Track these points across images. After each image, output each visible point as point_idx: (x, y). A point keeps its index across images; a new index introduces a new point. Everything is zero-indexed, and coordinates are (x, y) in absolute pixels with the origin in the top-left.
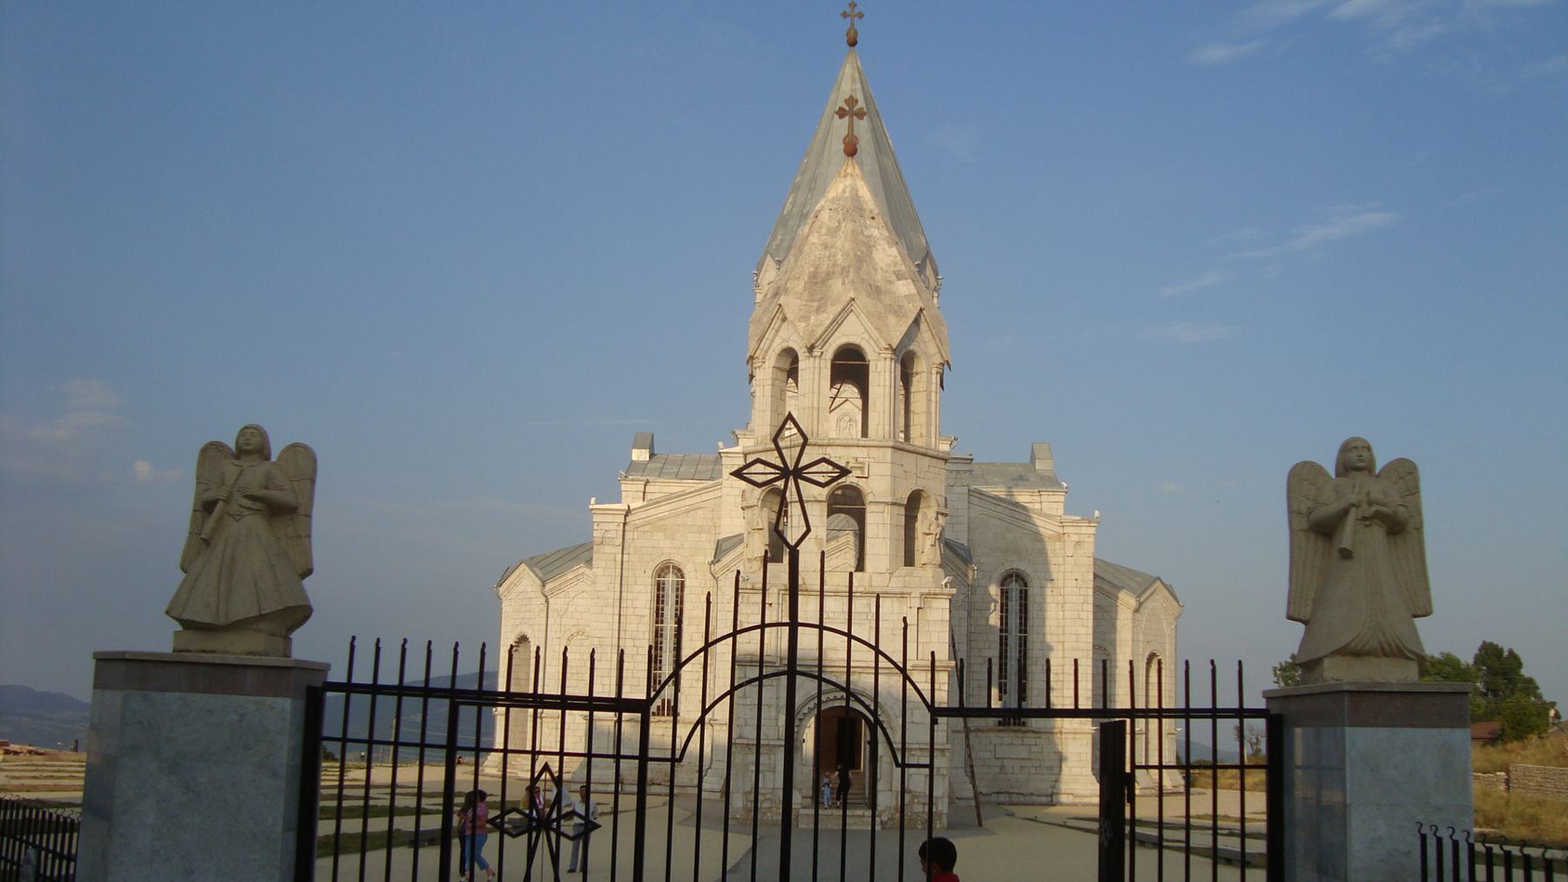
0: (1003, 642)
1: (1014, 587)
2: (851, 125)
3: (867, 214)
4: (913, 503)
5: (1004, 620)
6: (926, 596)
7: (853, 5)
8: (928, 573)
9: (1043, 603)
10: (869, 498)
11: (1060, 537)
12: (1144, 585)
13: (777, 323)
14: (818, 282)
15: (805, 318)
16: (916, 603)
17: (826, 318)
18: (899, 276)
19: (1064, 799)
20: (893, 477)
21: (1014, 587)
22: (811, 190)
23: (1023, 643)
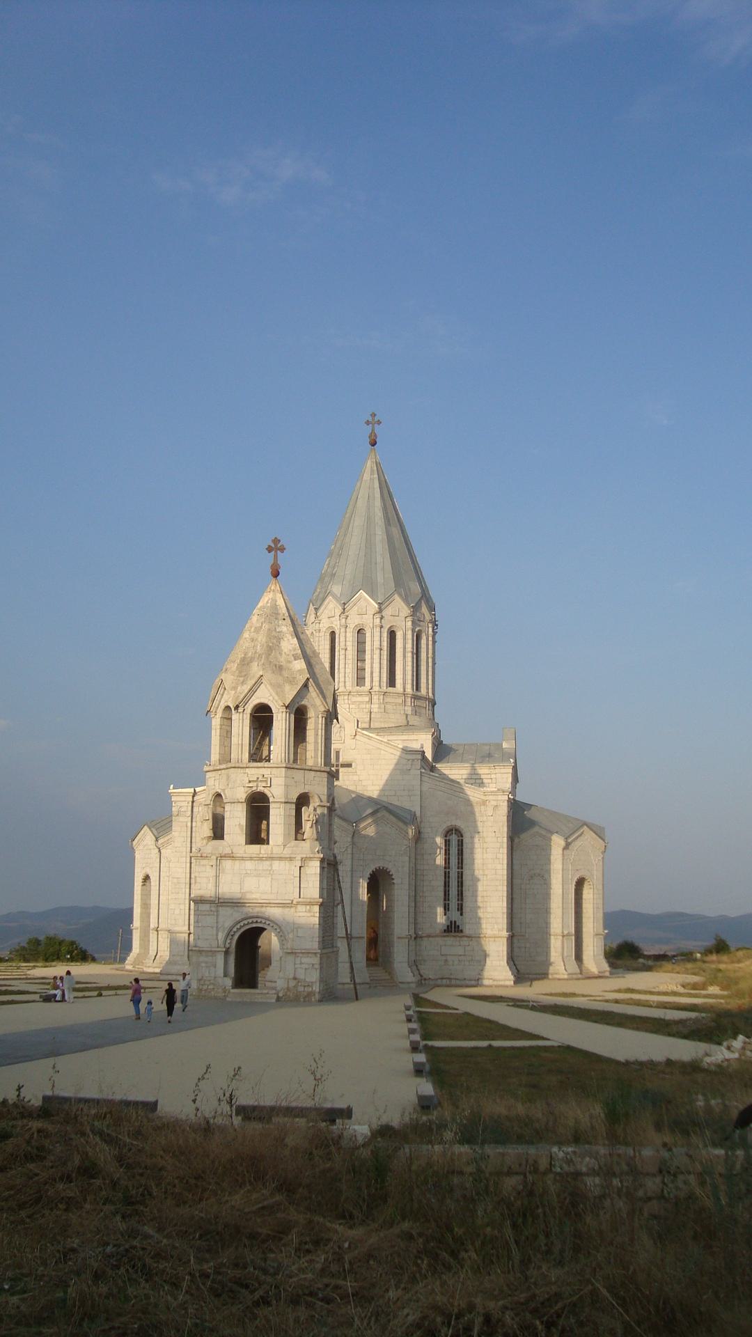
0: (447, 875)
1: (454, 839)
2: (276, 556)
3: (281, 617)
4: (303, 800)
5: (447, 861)
7: (374, 415)
8: (309, 847)
9: (472, 849)
10: (271, 800)
11: (484, 803)
12: (573, 828)
13: (221, 691)
14: (245, 663)
15: (235, 688)
17: (246, 688)
19: (486, 982)
20: (287, 786)
21: (454, 839)
22: (339, 555)
23: (460, 876)
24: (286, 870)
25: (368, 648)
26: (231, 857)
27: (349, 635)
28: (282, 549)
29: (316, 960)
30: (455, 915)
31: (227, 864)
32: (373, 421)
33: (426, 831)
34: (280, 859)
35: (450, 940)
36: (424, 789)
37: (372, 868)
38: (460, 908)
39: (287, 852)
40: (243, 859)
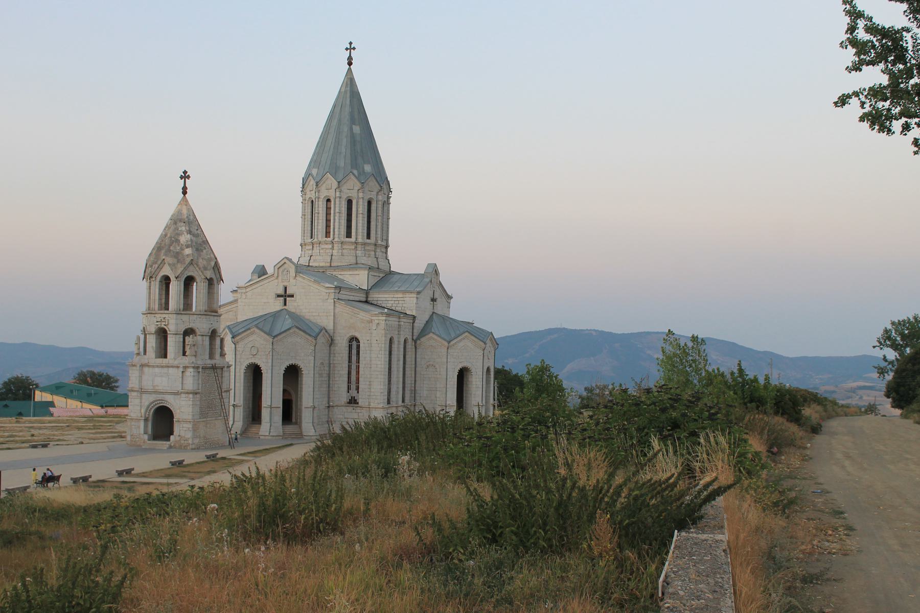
1: (354, 343)
6: (185, 367)
7: (351, 43)
16: (181, 370)
18: (187, 247)
21: (354, 343)
24: (176, 373)
25: (332, 212)
26: (149, 366)
27: (320, 203)
28: (189, 177)
29: (190, 426)
30: (353, 392)
31: (146, 369)
32: (350, 48)
33: (338, 339)
34: (172, 367)
35: (350, 409)
36: (337, 311)
37: (287, 364)
38: (358, 388)
39: (176, 363)
40: (153, 367)
